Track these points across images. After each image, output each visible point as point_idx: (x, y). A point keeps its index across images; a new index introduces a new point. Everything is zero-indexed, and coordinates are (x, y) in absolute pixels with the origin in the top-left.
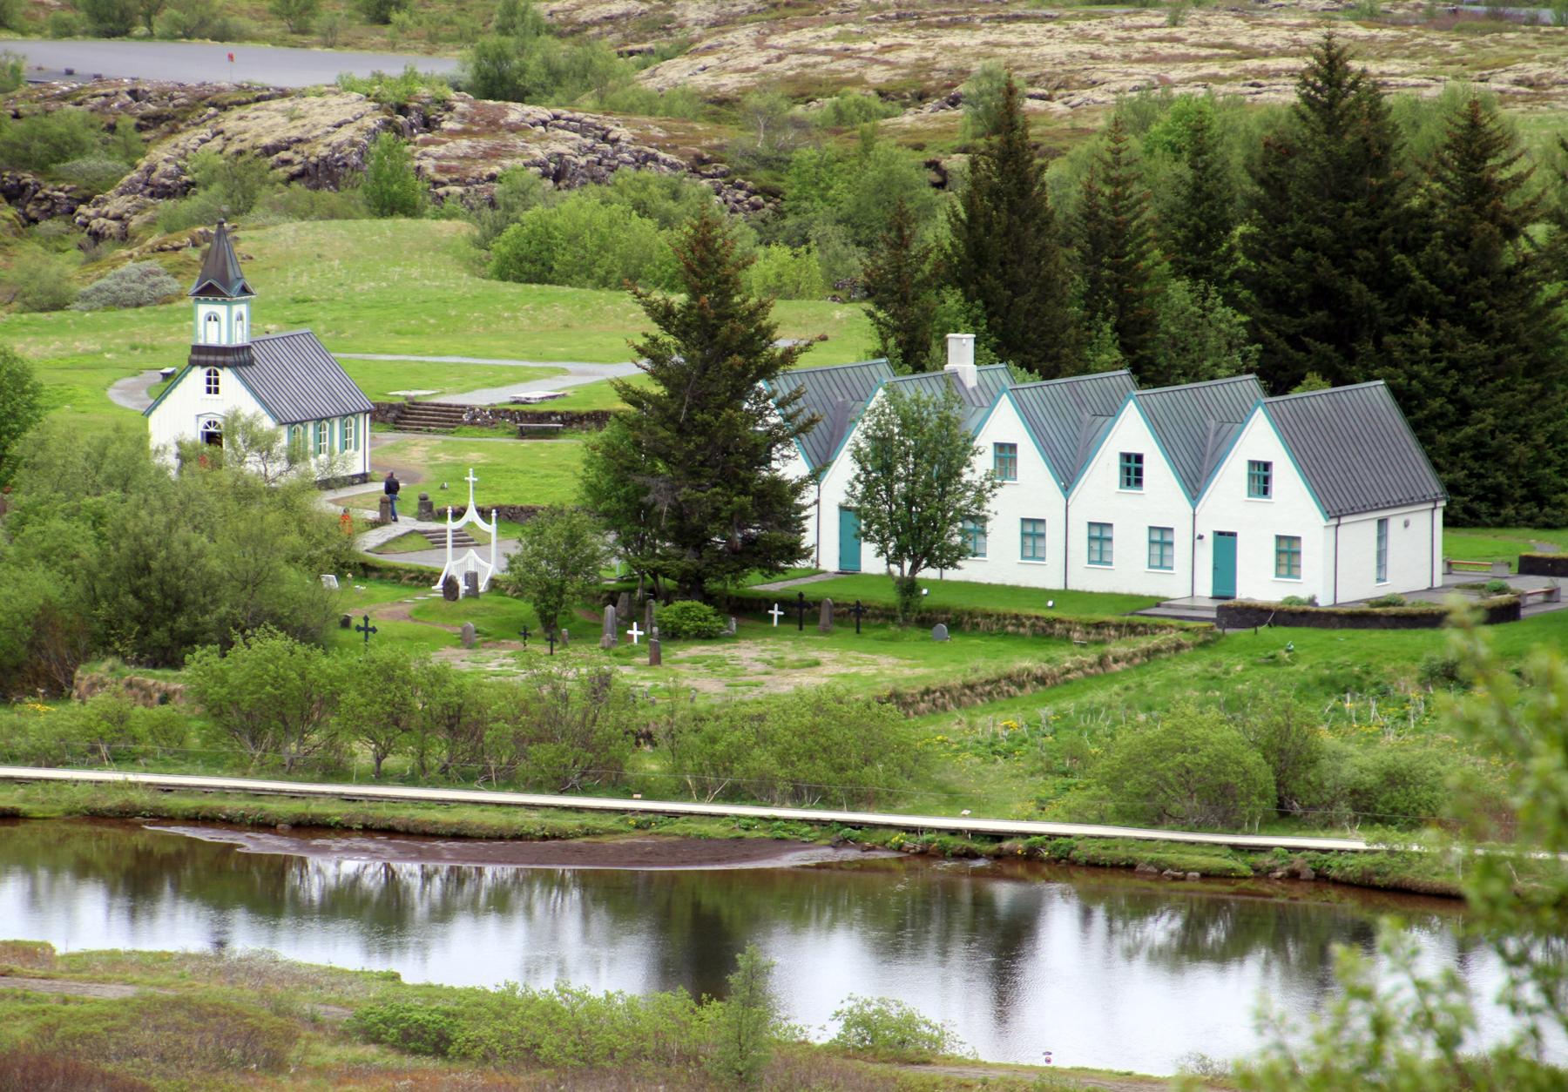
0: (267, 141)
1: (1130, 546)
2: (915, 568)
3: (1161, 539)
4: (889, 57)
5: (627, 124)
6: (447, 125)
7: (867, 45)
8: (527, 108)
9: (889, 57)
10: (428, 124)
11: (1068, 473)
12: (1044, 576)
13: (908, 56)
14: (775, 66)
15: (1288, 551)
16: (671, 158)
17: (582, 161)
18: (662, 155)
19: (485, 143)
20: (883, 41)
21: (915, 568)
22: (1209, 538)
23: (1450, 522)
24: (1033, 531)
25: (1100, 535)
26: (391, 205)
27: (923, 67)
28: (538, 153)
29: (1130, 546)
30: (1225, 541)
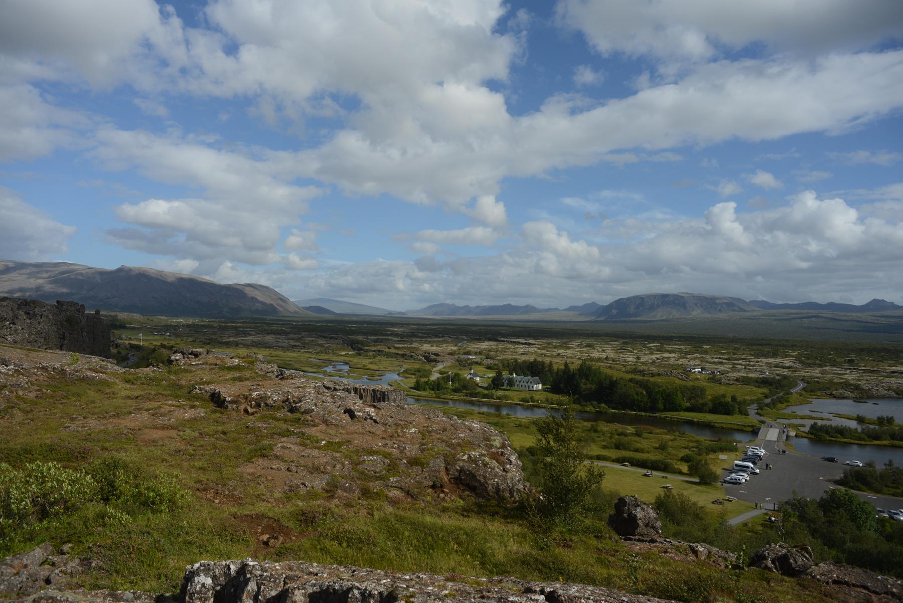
25: (522, 386)
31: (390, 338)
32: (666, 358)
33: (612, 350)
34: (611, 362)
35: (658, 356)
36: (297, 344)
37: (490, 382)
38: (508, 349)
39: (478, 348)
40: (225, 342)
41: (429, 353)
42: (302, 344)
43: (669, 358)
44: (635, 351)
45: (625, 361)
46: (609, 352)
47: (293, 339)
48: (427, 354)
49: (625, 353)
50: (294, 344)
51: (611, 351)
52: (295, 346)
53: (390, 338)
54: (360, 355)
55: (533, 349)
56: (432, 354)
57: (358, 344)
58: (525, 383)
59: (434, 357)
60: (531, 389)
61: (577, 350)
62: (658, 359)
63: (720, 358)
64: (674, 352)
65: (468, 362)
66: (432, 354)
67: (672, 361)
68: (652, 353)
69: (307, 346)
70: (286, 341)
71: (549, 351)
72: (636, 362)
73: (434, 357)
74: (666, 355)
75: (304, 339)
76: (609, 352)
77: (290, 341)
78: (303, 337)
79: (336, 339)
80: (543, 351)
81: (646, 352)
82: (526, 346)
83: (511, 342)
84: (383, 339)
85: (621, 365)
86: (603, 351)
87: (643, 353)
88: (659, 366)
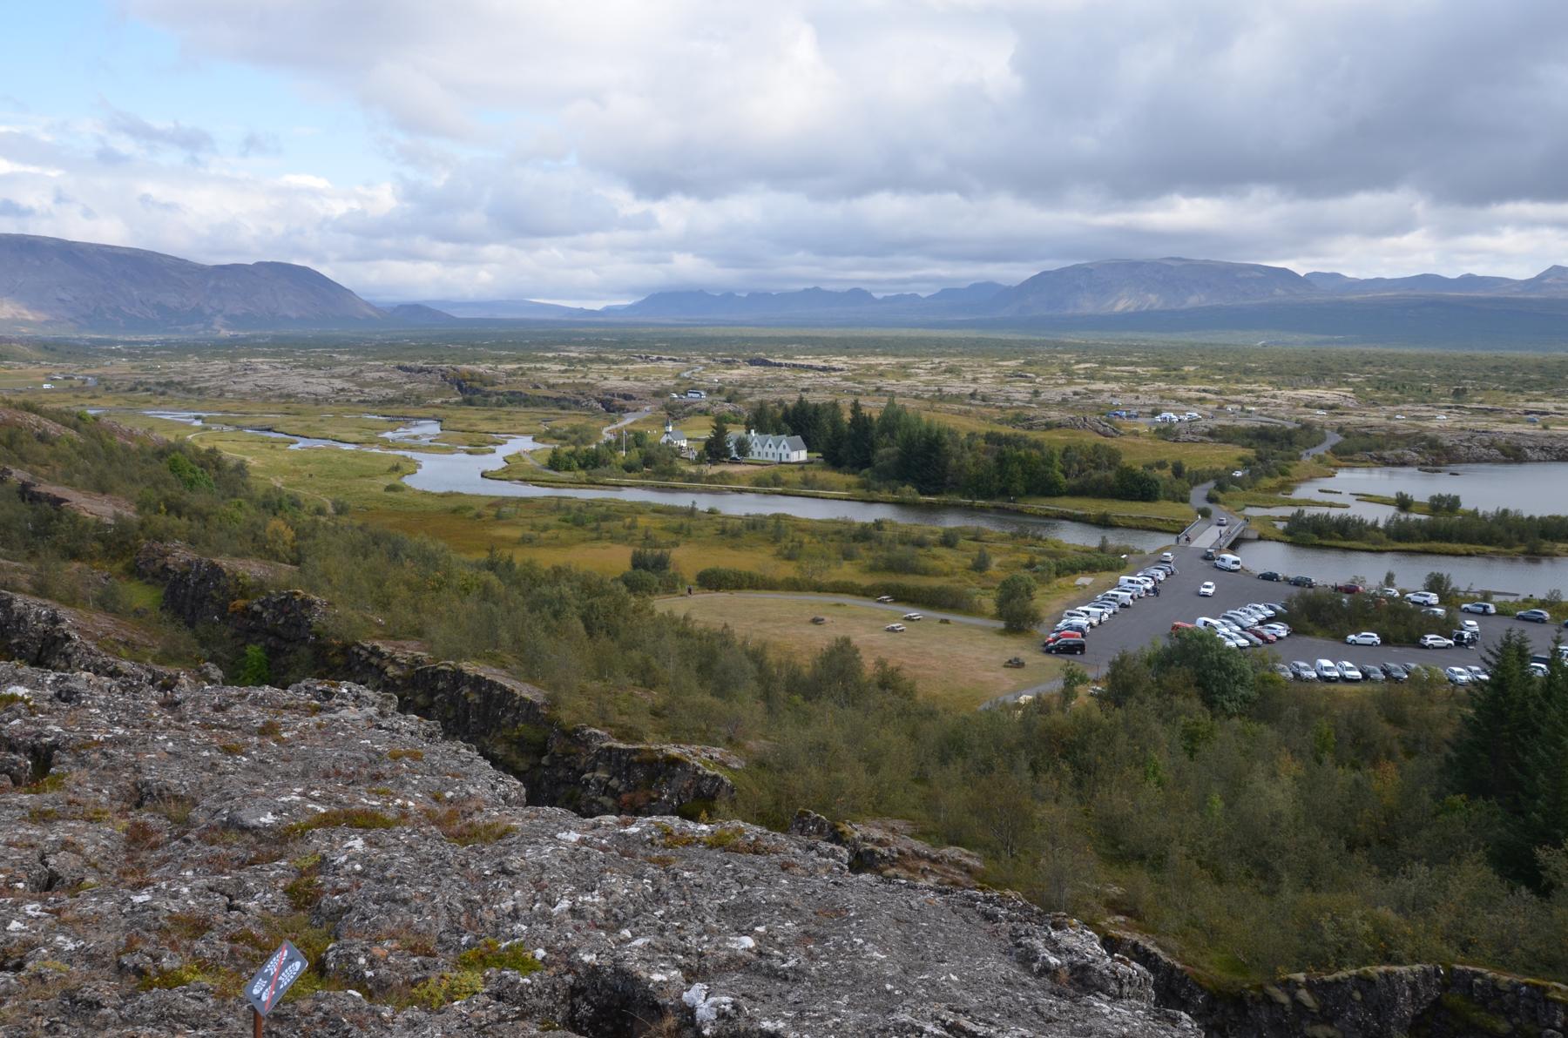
11: (763, 446)
12: (760, 458)
15: (788, 456)
26: (707, 415)
31: (546, 365)
32: (1093, 391)
33: (994, 377)
34: (977, 402)
35: (1078, 389)
36: (346, 385)
37: (702, 448)
38: (781, 381)
40: (199, 388)
41: (613, 395)
42: (358, 385)
43: (1101, 391)
44: (1037, 380)
45: (1008, 400)
46: (985, 381)
47: (340, 377)
48: (608, 397)
49: (1017, 384)
50: (340, 387)
51: (989, 381)
52: (343, 390)
53: (546, 365)
54: (470, 403)
55: (831, 380)
56: (619, 396)
57: (472, 380)
59: (624, 402)
60: (784, 459)
61: (922, 379)
62: (1076, 393)
63: (1205, 391)
64: (1117, 379)
65: (686, 410)
66: (619, 396)
67: (1105, 397)
68: (1070, 383)
69: (367, 390)
70: (325, 381)
72: (1030, 402)
73: (619, 402)
74: (1099, 385)
75: (362, 375)
76: (985, 381)
77: (333, 380)
78: (361, 371)
79: (430, 372)
80: (850, 384)
81: (1060, 382)
82: (822, 374)
83: (794, 365)
84: (529, 369)
85: (997, 407)
86: (975, 380)
87: (1052, 382)
88: (1073, 408)
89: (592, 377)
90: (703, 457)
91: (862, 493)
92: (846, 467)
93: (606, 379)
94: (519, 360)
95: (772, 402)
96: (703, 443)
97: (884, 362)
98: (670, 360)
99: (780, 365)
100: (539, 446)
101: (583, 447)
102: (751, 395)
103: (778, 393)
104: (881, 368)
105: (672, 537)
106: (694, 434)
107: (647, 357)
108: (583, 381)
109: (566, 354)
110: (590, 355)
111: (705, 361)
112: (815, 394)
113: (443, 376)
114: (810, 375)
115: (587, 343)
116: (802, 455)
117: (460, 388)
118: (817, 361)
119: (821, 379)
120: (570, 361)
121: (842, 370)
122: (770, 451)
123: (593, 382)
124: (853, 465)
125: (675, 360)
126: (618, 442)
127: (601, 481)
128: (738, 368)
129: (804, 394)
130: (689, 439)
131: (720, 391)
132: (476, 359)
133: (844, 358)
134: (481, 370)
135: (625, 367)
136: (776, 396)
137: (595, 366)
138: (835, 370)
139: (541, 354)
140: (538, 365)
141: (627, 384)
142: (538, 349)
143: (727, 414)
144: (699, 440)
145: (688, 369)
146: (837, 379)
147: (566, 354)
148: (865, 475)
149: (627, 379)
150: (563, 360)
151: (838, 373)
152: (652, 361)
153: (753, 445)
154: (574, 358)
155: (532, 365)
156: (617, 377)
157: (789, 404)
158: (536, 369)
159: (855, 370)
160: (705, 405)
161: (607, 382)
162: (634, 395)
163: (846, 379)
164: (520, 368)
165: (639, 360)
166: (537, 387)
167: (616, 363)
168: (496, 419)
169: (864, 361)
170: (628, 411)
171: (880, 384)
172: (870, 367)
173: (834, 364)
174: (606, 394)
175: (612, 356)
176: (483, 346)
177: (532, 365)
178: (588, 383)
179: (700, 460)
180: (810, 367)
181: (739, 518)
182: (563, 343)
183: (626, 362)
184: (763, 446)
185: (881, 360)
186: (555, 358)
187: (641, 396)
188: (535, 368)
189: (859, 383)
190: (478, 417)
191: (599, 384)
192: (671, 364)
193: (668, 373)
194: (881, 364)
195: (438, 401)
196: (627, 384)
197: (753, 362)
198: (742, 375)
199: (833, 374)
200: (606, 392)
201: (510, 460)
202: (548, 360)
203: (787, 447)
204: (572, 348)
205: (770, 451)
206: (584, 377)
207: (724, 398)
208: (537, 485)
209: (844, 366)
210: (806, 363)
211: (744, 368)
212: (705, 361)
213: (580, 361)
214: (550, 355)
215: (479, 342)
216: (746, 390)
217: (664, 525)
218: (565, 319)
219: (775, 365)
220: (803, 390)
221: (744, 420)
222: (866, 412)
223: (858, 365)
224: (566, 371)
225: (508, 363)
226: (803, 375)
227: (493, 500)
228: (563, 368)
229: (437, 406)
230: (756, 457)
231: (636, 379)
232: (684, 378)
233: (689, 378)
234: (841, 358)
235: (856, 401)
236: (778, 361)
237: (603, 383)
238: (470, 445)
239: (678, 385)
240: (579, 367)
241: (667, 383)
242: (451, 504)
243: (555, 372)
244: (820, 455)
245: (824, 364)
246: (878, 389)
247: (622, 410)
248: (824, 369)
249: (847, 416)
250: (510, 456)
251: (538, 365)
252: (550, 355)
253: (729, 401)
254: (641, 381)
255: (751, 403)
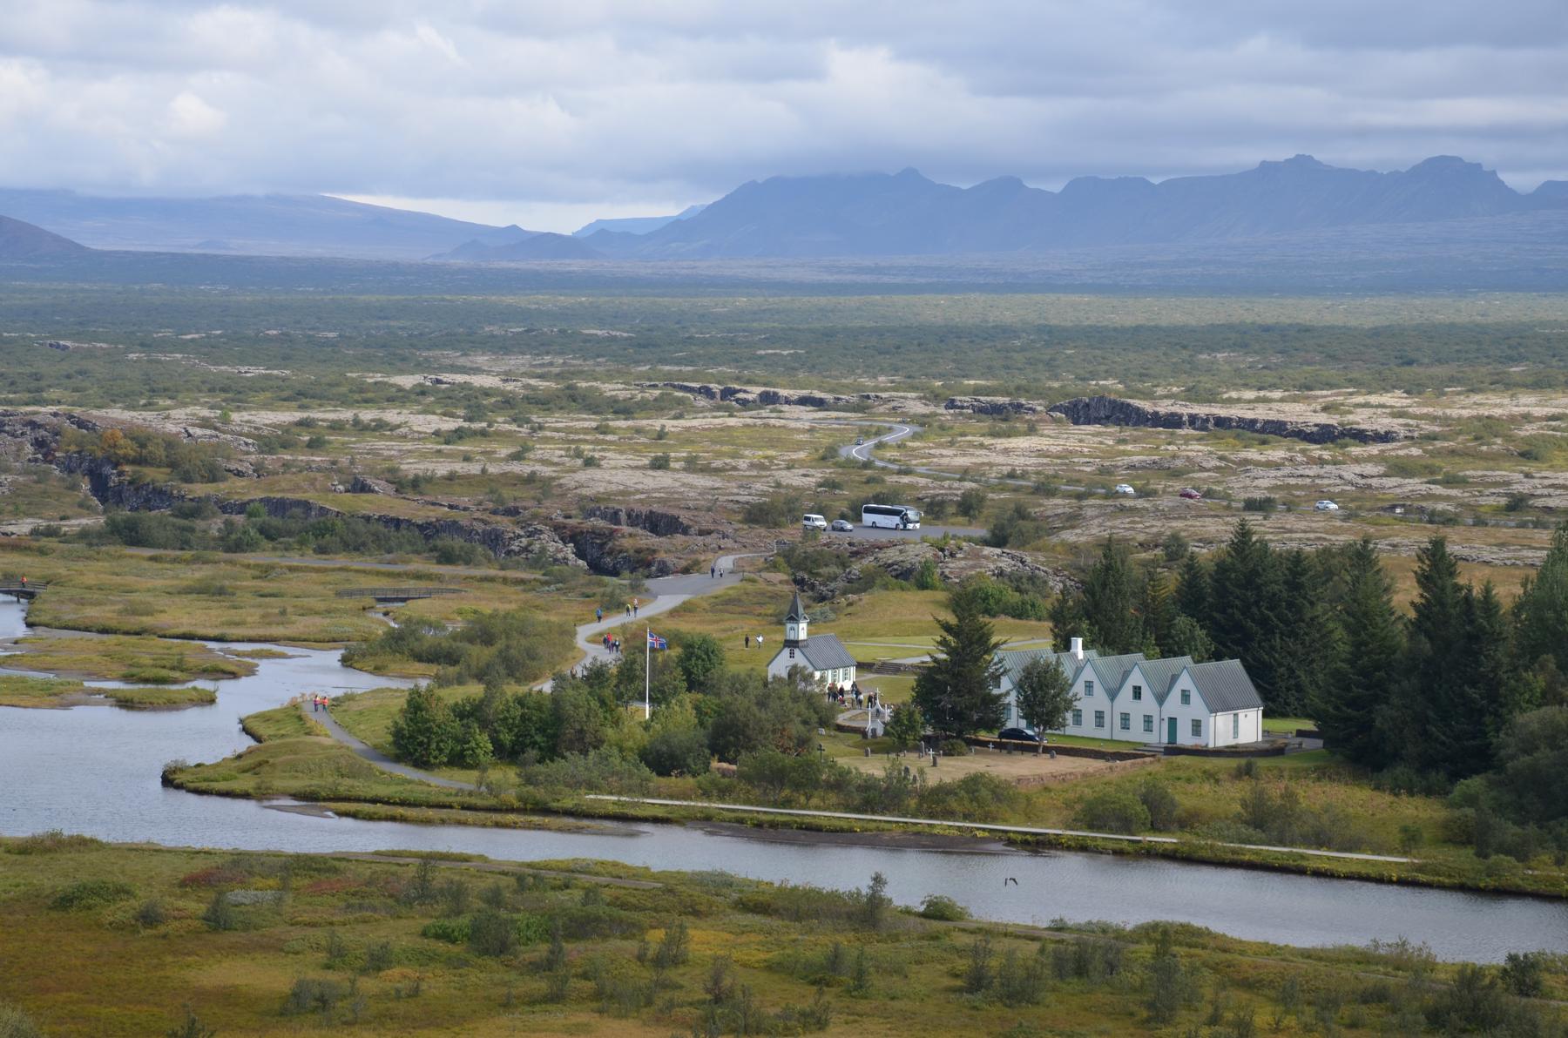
0: (890, 561)
1: (1137, 723)
2: (1044, 730)
3: (1148, 720)
4: (1147, 530)
5: (1030, 555)
6: (958, 556)
7: (1141, 526)
8: (992, 549)
9: (1147, 530)
10: (952, 555)
13: (1155, 530)
14: (1102, 533)
15: (1197, 727)
16: (1045, 569)
17: (1009, 570)
18: (1042, 568)
19: (971, 563)
20: (1147, 524)
21: (1044, 730)
22: (1167, 720)
23: (1265, 715)
24: (1099, 716)
25: (1125, 718)
26: (923, 586)
27: (1160, 534)
28: (992, 567)
29: (1137, 723)
30: (1172, 721)
31: (391, 416)
37: (907, 696)
38: (1176, 474)
39: (965, 474)
41: (614, 517)
48: (601, 523)
53: (391, 416)
54: (132, 535)
55: (1350, 471)
56: (633, 519)
57: (140, 461)
58: (1148, 703)
59: (646, 539)
60: (1185, 738)
65: (856, 568)
66: (633, 519)
71: (1461, 482)
73: (633, 539)
80: (1415, 485)
82: (1316, 450)
83: (1221, 422)
84: (336, 427)
89: (546, 458)
90: (912, 727)
91: (1462, 859)
92: (1401, 771)
93: (590, 463)
94: (300, 396)
95: (1143, 546)
96: (911, 680)
97: (1538, 411)
98: (803, 401)
99: (1173, 421)
100: (362, 682)
101: (512, 689)
102: (1073, 520)
103: (1165, 516)
104: (1529, 430)
105: (804, 998)
106: (877, 650)
107: (728, 393)
108: (516, 468)
109: (460, 378)
110: (543, 384)
111: (919, 408)
112: (1290, 521)
113: (39, 444)
114: (1277, 454)
115: (532, 341)
116: (1249, 726)
117: (100, 487)
118: (1298, 408)
119: (1314, 470)
120: (473, 402)
121: (1386, 437)
122: (1137, 711)
123: (547, 471)
124: (1426, 764)
125: (819, 404)
126: (628, 673)
127: (568, 803)
128: (1031, 430)
129: (1254, 520)
130: (861, 666)
131: (968, 507)
132: (155, 390)
133: (1395, 399)
134: (171, 428)
135: (657, 424)
136: (1157, 526)
137: (557, 420)
138: (1361, 437)
139: (379, 377)
140: (367, 415)
141: (663, 480)
142: (367, 362)
143: (992, 584)
144: (897, 669)
145: (865, 433)
146: (1369, 469)
147: (460, 378)
148: (1471, 800)
149: (660, 464)
150: (448, 399)
151: (1374, 449)
152: (744, 403)
153: (1079, 688)
154: (487, 393)
155: (346, 415)
156: (622, 460)
157: (1204, 553)
158: (360, 427)
159: (1432, 437)
160: (916, 553)
161: (591, 473)
162: (684, 517)
163: (1401, 469)
164: (305, 424)
165: (702, 402)
166: (360, 487)
167: (624, 409)
168: (221, 592)
169: (1464, 407)
170: (664, 571)
171: (1522, 487)
172: (1488, 427)
173: (1361, 419)
174: (592, 514)
175: (613, 389)
176: (183, 347)
177: (346, 415)
178: (531, 479)
179: (899, 737)
180: (1277, 430)
181: (1030, 936)
182: (451, 341)
183: (657, 407)
184: (1113, 694)
185: (1527, 403)
186: (422, 391)
187: (705, 521)
188: (357, 422)
189: (1450, 481)
190: (159, 583)
191: (568, 480)
192: (807, 415)
193: (799, 446)
194: (1527, 418)
195: (23, 527)
196: (663, 480)
197: (1080, 412)
198: (1041, 454)
199: (1356, 450)
200: (591, 506)
201: (262, 730)
202: (400, 398)
203: (1195, 697)
204: (481, 360)
205: (1137, 711)
206: (517, 457)
207: (981, 531)
208: (354, 815)
209: (1395, 425)
210: (1261, 413)
211: (1049, 429)
212: (919, 408)
213: (507, 402)
214: (407, 381)
215: (168, 333)
216: (1056, 505)
217: (775, 955)
218: (459, 262)
219: (1157, 420)
220: (1252, 505)
221: (1047, 605)
222: (1471, 579)
223: (1446, 421)
224: (459, 435)
225: (266, 406)
226: (1252, 454)
227: (199, 865)
228: (449, 425)
229: (16, 547)
230: (1088, 728)
231: (692, 465)
232: (851, 464)
233: (867, 465)
234: (1386, 399)
235: (1438, 544)
236: (1164, 408)
237: (582, 476)
238: (127, 678)
239: (831, 485)
240: (502, 424)
241: (794, 479)
242: (51, 878)
243: (421, 437)
244: (1309, 725)
245: (1323, 419)
246: (1517, 504)
247: (644, 565)
248: (1324, 435)
249: (1405, 595)
250: (265, 717)
251: (367, 415)
252: (407, 381)
253: (998, 540)
254: (706, 470)
255: (1074, 549)
